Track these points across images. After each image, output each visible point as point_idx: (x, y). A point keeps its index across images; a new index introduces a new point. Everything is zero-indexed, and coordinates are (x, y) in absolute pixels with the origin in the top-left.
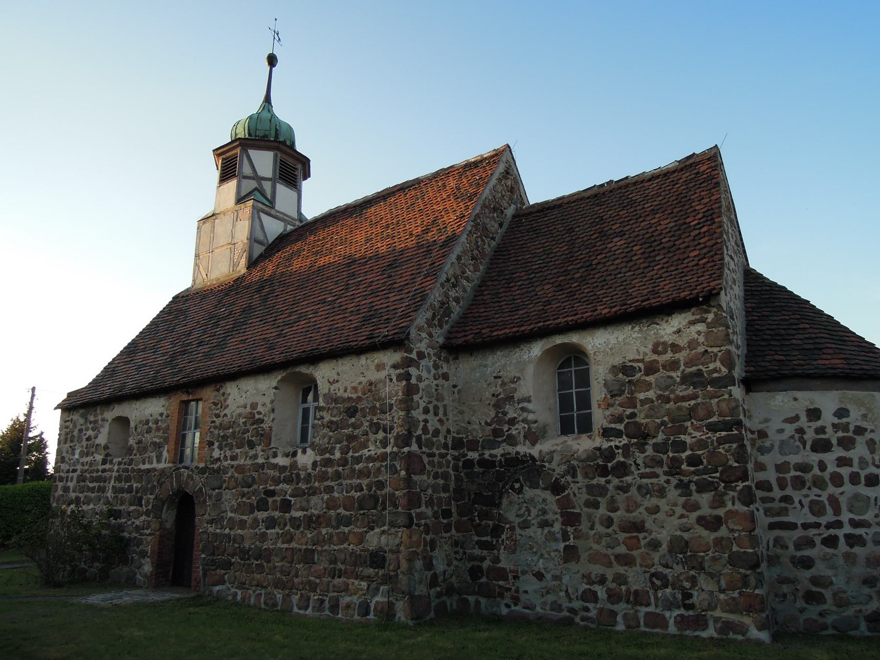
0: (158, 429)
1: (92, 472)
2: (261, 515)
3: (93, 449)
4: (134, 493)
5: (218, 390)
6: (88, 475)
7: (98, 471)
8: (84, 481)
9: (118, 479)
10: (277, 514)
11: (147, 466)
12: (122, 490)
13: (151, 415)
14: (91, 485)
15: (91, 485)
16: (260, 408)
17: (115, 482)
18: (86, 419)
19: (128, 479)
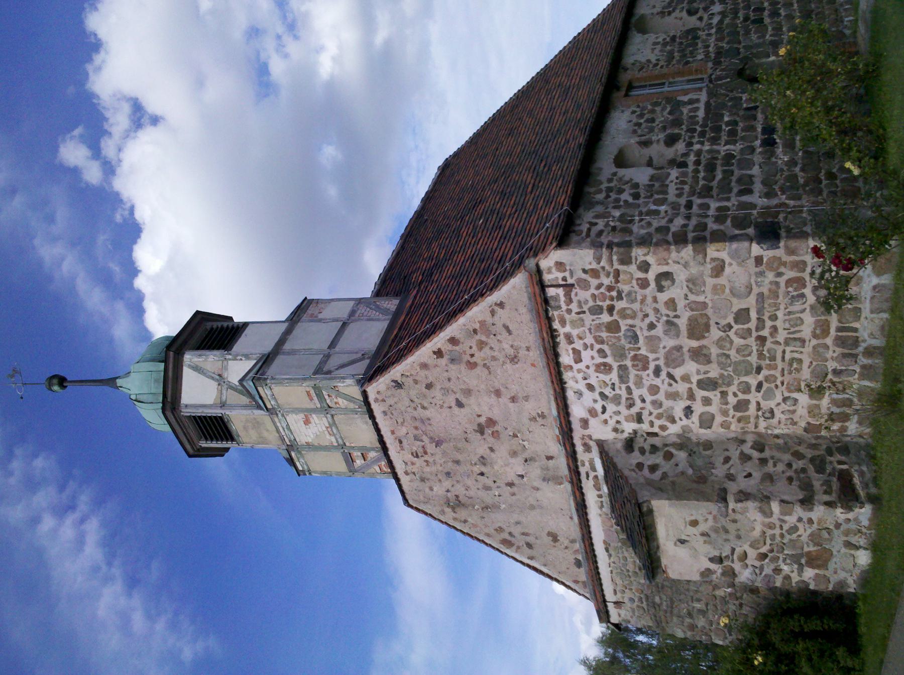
0: (652, 111)
1: (696, 179)
2: (767, 20)
3: (657, 185)
4: (738, 119)
5: (626, 69)
6: (701, 183)
7: (697, 171)
8: (711, 188)
9: (715, 140)
10: (766, 13)
11: (701, 114)
12: (732, 133)
13: (630, 121)
14: (719, 176)
15: (719, 176)
16: (660, 40)
17: (719, 144)
18: (598, 203)
19: (718, 129)
